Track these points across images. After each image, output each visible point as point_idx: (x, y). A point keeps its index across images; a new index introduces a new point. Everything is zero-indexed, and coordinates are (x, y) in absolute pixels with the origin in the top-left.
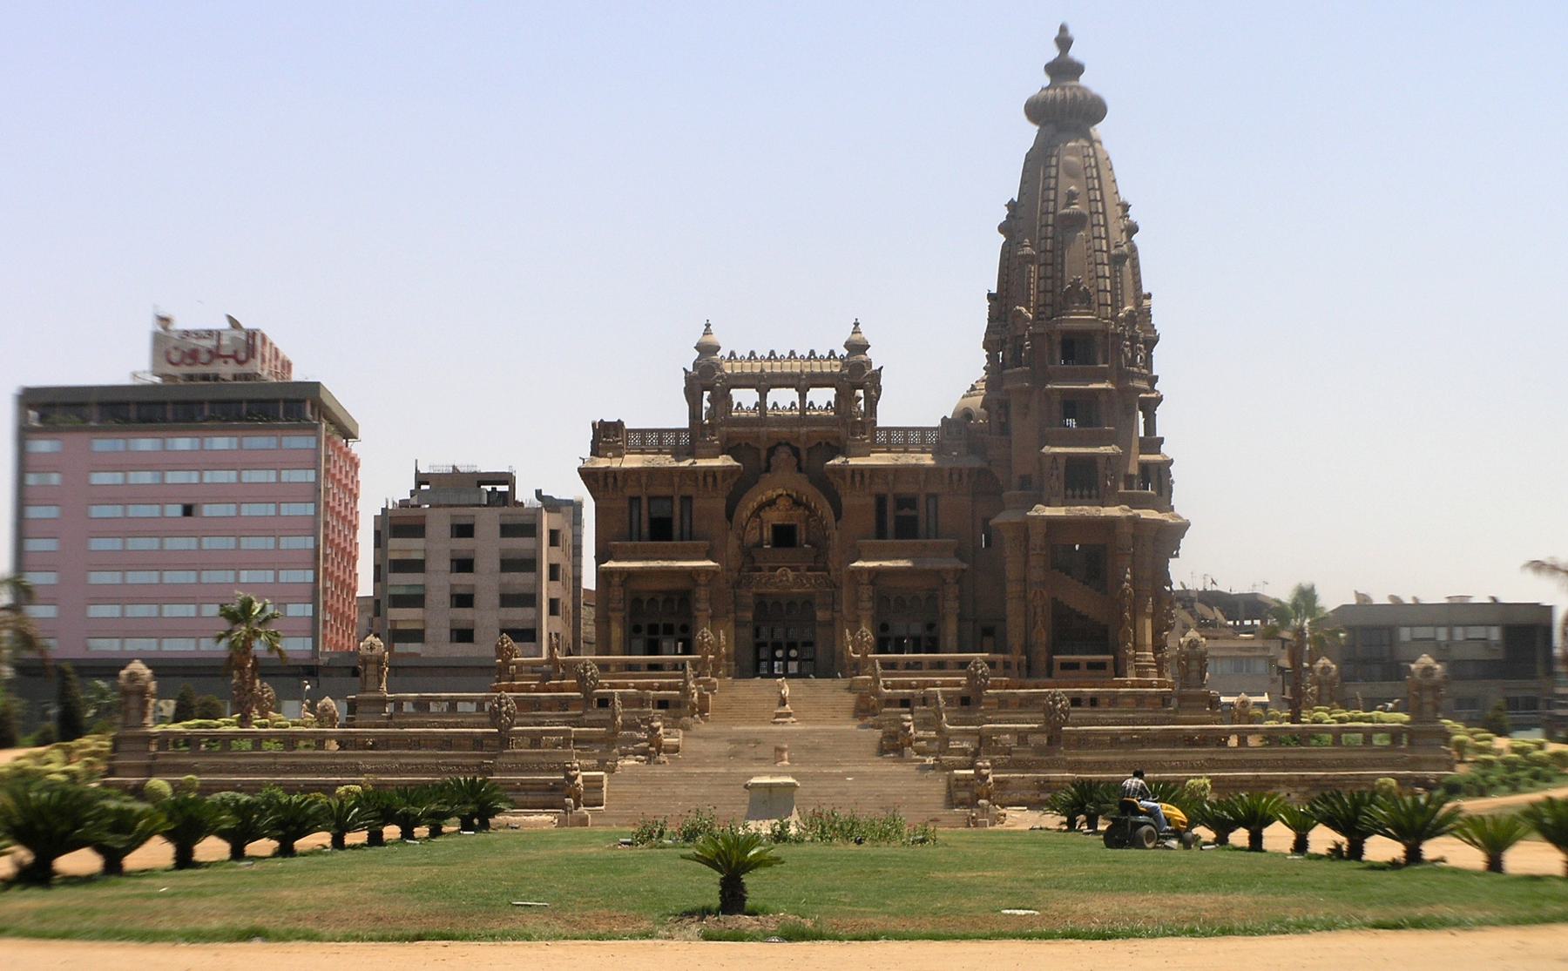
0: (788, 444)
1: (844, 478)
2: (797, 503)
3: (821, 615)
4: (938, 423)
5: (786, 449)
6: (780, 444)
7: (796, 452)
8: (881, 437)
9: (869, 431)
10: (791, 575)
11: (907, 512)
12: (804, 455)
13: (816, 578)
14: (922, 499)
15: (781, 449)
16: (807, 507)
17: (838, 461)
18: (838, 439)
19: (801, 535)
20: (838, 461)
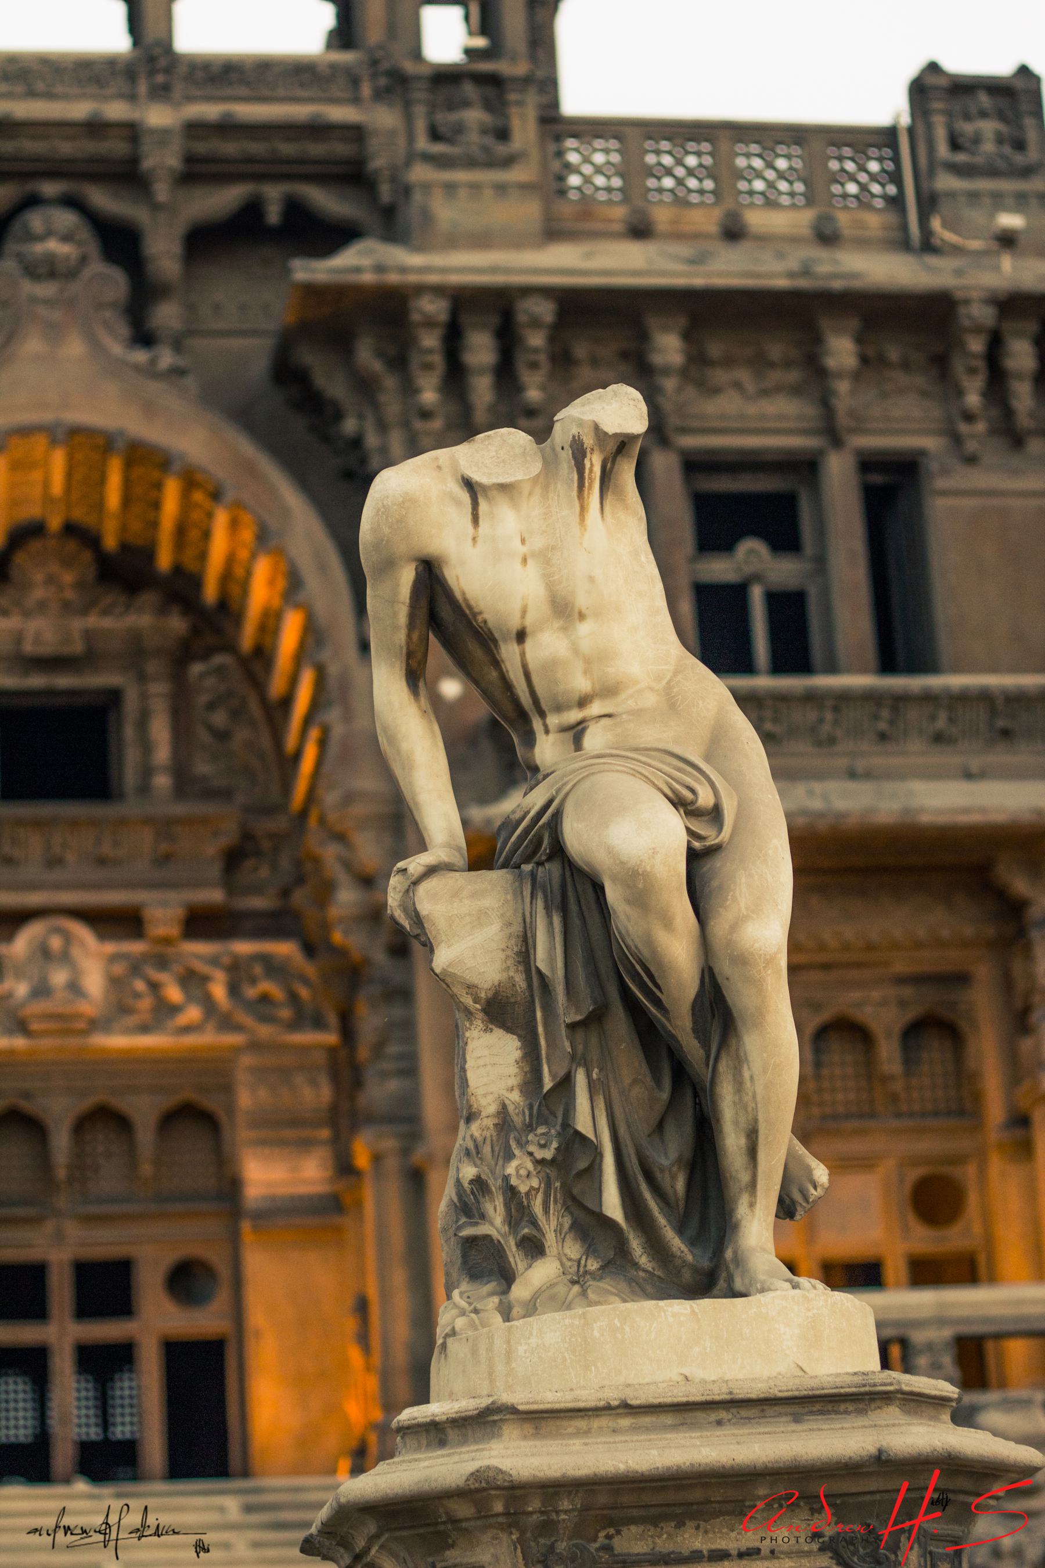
0: (71, 202)
1: (399, 362)
2: (123, 571)
3: (266, 1174)
4: (886, 106)
5: (66, 219)
6: (32, 201)
7: (120, 243)
8: (591, 168)
9: (524, 130)
10: (92, 965)
11: (751, 559)
12: (164, 251)
13: (238, 973)
14: (839, 472)
15: (35, 220)
16: (181, 589)
17: (357, 262)
18: (354, 176)
19: (151, 741)
20: (357, 262)
